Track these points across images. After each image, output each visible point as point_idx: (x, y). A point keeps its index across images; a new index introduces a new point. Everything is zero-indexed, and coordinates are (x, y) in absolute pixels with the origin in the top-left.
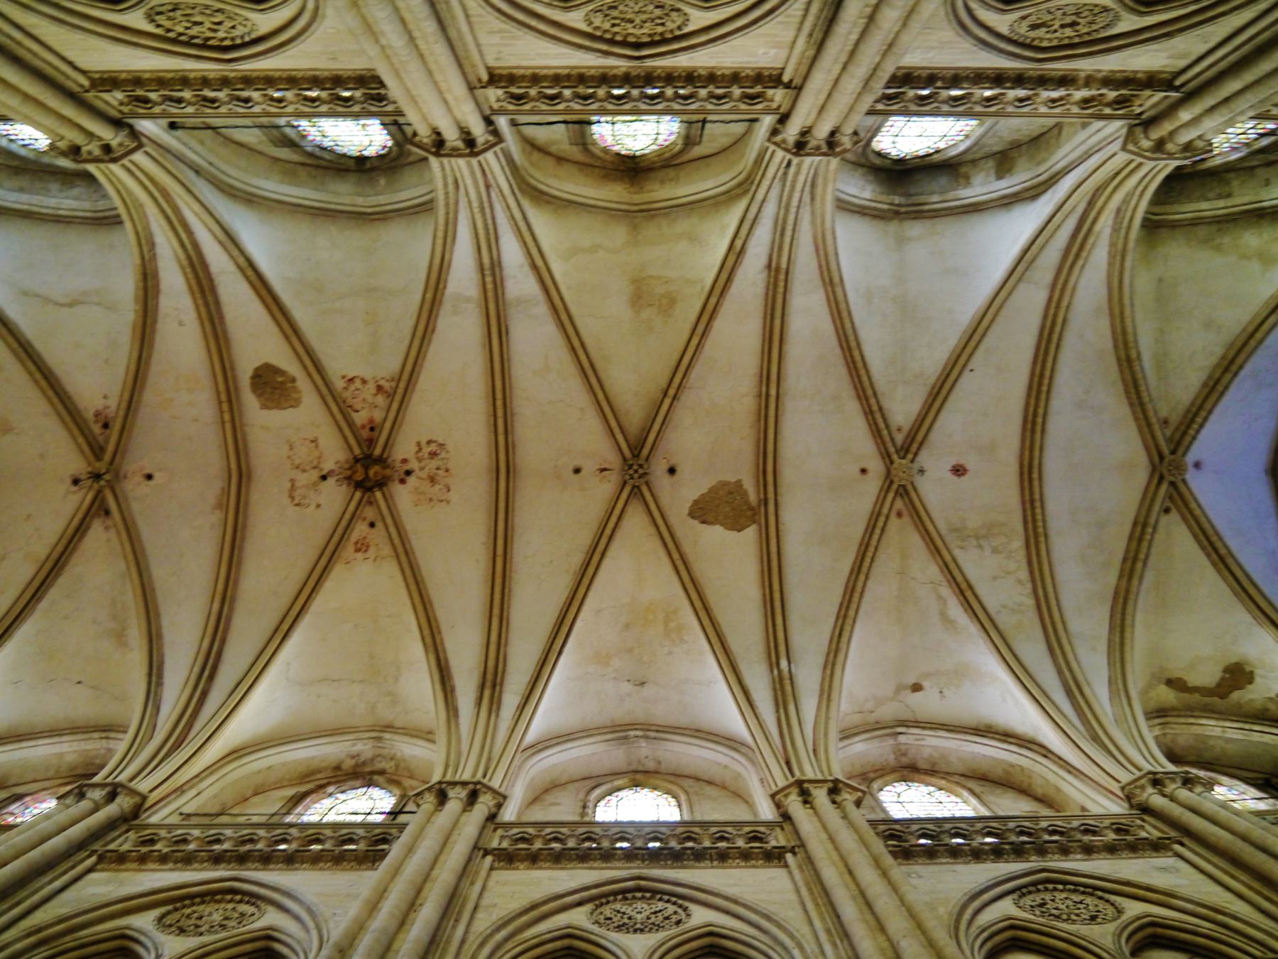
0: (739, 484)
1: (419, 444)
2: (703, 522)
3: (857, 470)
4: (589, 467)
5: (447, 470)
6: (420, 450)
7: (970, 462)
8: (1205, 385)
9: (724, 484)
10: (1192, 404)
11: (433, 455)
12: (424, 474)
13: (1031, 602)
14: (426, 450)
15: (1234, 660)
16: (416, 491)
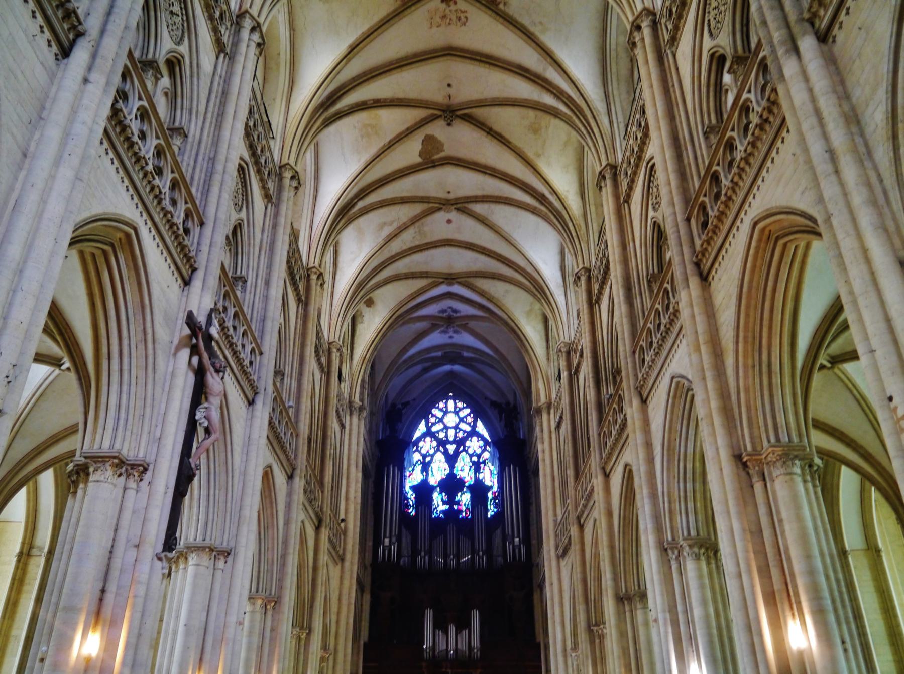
0: (443, 150)
1: (466, 12)
2: (423, 141)
3: (448, 190)
4: (451, 91)
5: (449, 24)
6: (462, 12)
7: (451, 225)
8: (483, 291)
9: (443, 145)
10: (476, 286)
11: (459, 19)
12: (447, 11)
13: (393, 253)
14: (462, 16)
15: (375, 300)
16: (437, 10)
